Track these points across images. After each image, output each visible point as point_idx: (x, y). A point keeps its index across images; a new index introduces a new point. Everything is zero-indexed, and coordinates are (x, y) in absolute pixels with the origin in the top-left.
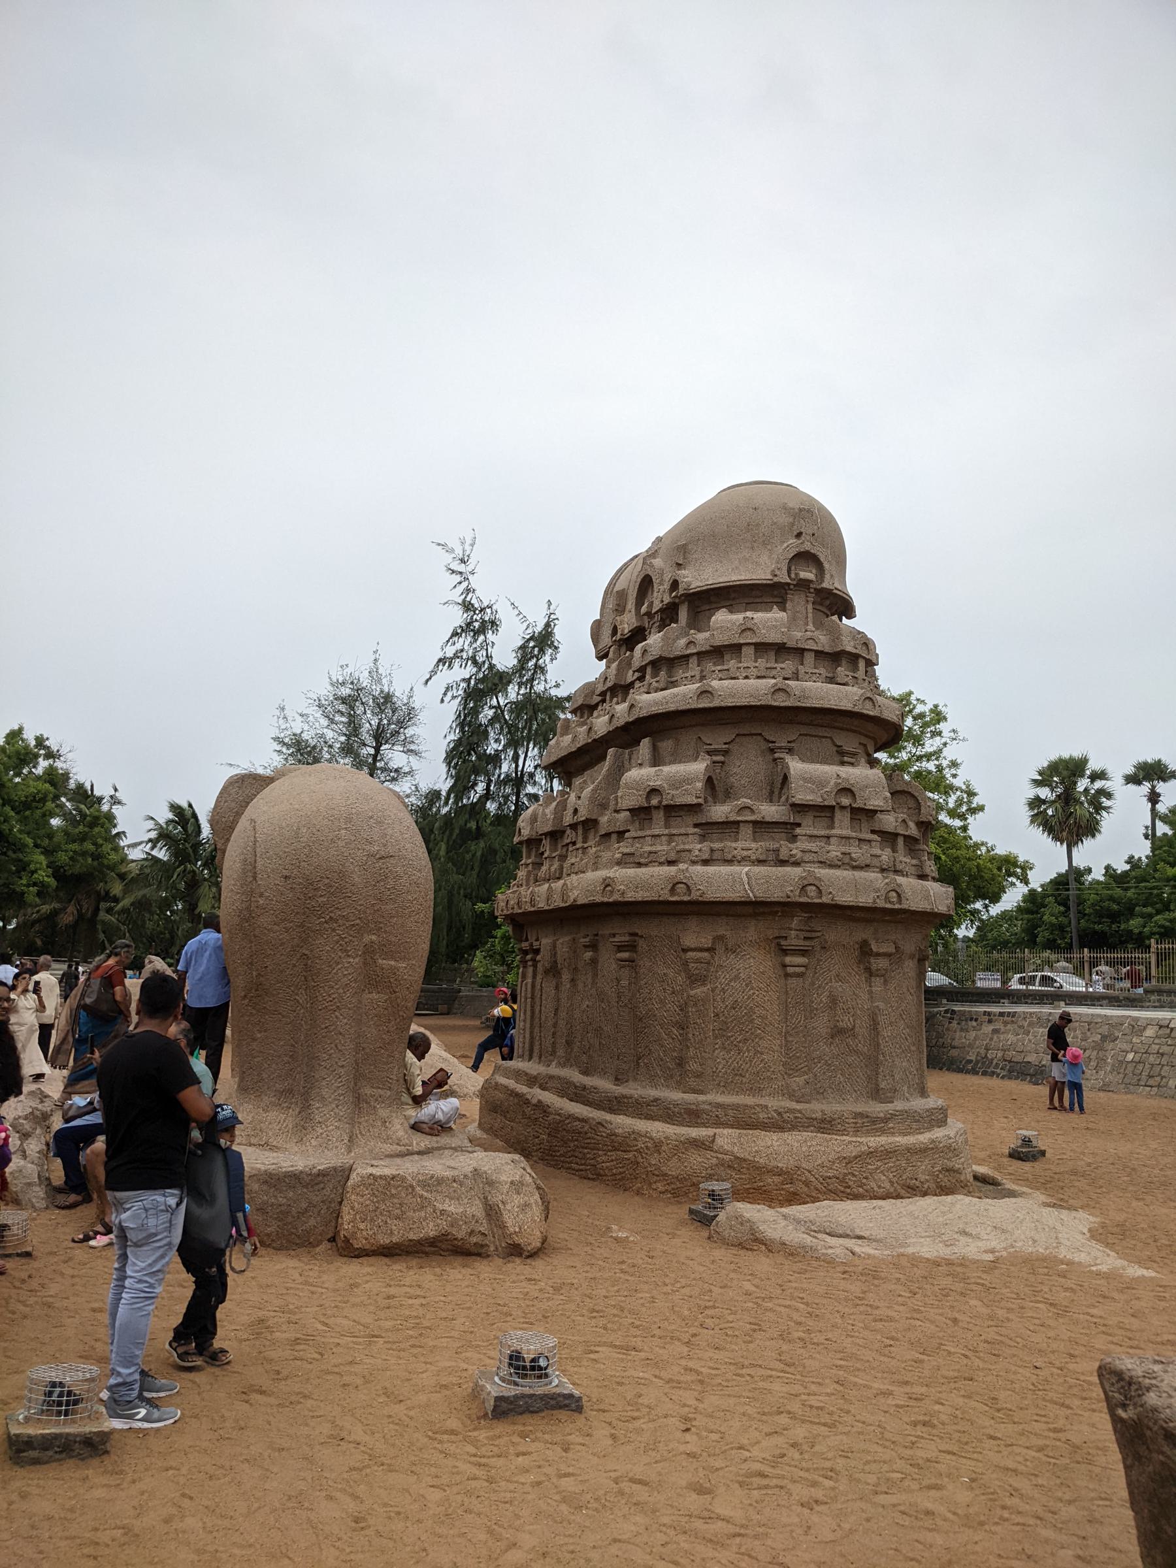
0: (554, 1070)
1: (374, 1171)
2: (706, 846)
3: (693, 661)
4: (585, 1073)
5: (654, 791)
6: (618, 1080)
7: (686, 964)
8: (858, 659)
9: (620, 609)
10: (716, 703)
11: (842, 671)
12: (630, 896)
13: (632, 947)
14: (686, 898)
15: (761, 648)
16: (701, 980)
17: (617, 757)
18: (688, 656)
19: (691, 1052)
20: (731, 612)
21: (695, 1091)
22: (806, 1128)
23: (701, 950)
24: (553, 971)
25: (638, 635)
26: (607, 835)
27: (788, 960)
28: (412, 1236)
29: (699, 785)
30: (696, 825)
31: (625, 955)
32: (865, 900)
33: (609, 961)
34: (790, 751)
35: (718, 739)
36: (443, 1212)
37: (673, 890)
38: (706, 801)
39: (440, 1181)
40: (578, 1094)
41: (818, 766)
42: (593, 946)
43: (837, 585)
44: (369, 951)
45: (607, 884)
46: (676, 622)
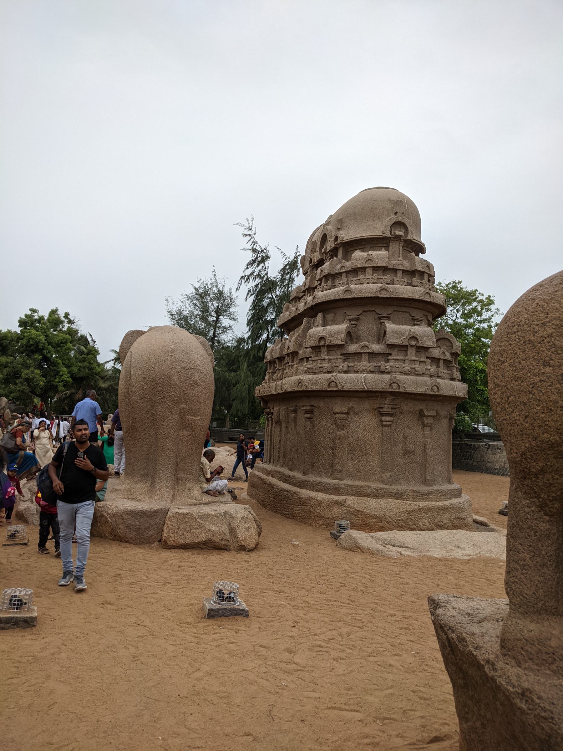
0: (278, 469)
1: (180, 511)
2: (346, 364)
4: (291, 470)
5: (322, 338)
6: (304, 474)
7: (335, 420)
8: (425, 274)
9: (313, 251)
10: (353, 296)
11: (415, 280)
12: (310, 388)
13: (311, 412)
14: (335, 389)
15: (376, 269)
16: (342, 427)
17: (308, 322)
18: (340, 274)
19: (337, 461)
20: (363, 251)
21: (338, 479)
22: (389, 497)
23: (342, 413)
24: (279, 423)
25: (321, 262)
26: (302, 359)
27: (383, 418)
29: (343, 335)
30: (342, 355)
31: (308, 415)
32: (421, 390)
33: (302, 417)
34: (389, 319)
35: (354, 313)
36: (209, 530)
37: (329, 385)
39: (209, 516)
40: (286, 479)
41: (401, 326)
42: (295, 411)
43: (415, 238)
44: (182, 413)
45: (300, 382)
46: (337, 256)
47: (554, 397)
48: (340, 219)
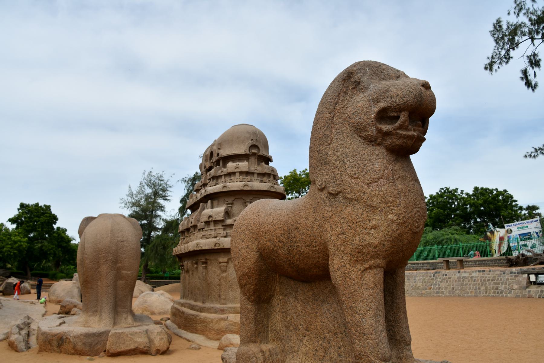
0: (188, 301)
1: (117, 331)
2: (225, 232)
3: (223, 177)
4: (195, 301)
5: (210, 216)
6: (203, 303)
7: (220, 267)
9: (206, 161)
12: (204, 248)
15: (241, 173)
16: (225, 271)
17: (203, 206)
18: (222, 176)
19: (222, 293)
20: (234, 162)
21: (223, 304)
25: (210, 168)
26: (199, 230)
28: (127, 349)
29: (223, 214)
30: (223, 226)
31: (204, 265)
33: (201, 267)
36: (136, 341)
37: (215, 246)
38: (225, 218)
39: (136, 333)
40: (192, 308)
42: (196, 263)
43: (265, 153)
47: (245, 254)
48: (220, 143)
